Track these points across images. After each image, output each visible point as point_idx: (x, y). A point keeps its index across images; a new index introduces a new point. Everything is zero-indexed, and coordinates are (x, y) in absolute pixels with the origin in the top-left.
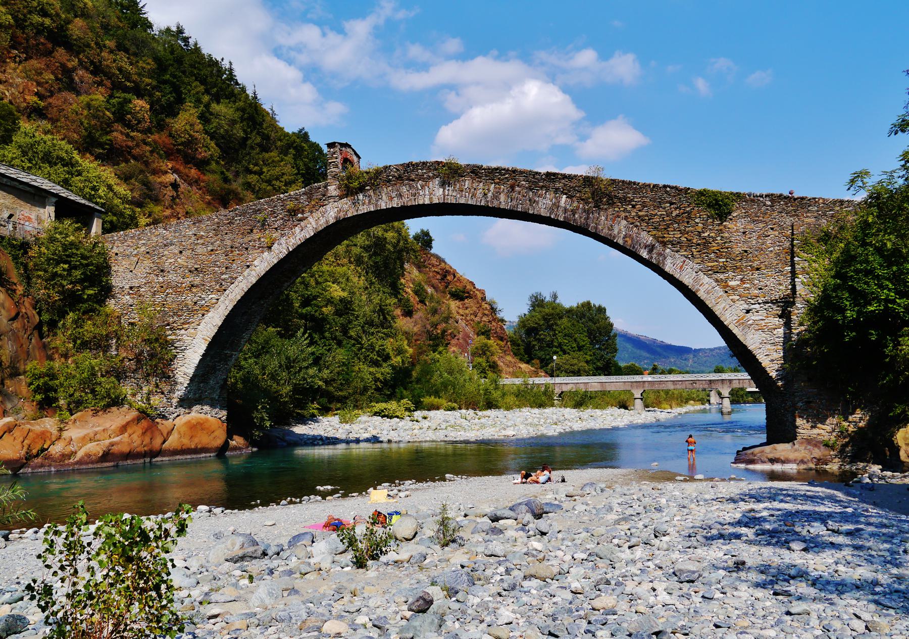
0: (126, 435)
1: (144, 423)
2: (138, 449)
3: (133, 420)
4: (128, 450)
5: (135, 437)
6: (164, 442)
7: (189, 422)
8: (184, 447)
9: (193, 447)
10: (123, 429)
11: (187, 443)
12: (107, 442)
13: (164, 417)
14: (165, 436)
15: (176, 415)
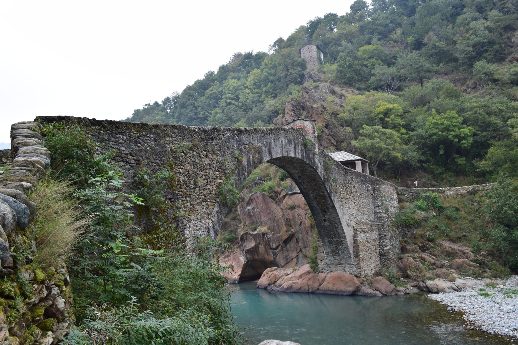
0: (301, 279)
1: (311, 275)
2: (305, 287)
3: (305, 273)
4: (299, 287)
5: (304, 280)
6: (320, 285)
7: (333, 276)
8: (329, 289)
9: (334, 289)
10: (300, 277)
11: (331, 286)
12: (291, 282)
13: (323, 272)
14: (320, 281)
15: (329, 271)
